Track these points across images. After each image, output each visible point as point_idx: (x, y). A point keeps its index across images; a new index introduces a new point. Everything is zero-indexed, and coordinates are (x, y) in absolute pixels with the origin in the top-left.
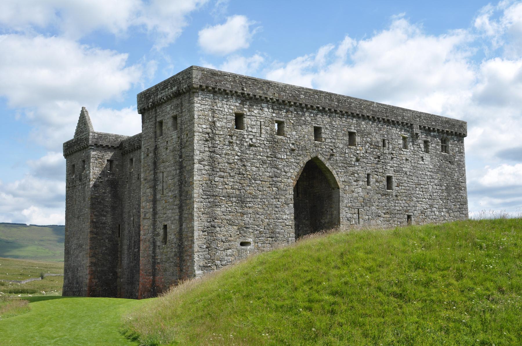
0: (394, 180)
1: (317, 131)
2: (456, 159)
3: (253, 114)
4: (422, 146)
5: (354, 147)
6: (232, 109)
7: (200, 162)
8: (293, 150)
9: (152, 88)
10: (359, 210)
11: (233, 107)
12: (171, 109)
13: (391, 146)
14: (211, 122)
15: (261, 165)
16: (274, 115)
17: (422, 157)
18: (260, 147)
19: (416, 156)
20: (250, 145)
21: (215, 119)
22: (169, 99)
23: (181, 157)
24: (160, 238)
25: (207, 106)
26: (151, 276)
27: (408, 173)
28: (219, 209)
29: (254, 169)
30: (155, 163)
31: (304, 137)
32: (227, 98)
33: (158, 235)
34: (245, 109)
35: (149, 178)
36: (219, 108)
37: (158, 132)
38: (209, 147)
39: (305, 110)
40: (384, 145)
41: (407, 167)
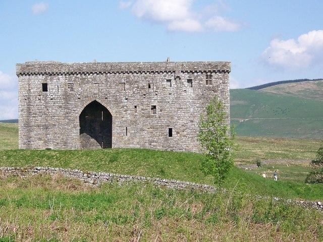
4: (186, 84)
29: (54, 111)
40: (149, 87)
41: (170, 99)
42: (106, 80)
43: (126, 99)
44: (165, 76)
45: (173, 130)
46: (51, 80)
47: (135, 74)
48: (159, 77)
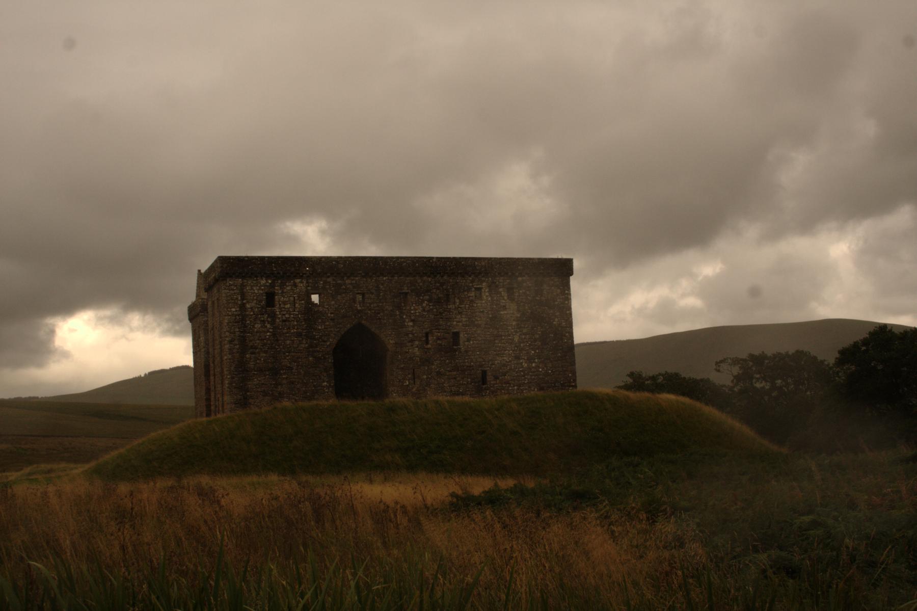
0: (461, 335)
2: (556, 303)
3: (285, 291)
6: (262, 290)
7: (231, 342)
8: (332, 319)
10: (415, 370)
11: (263, 288)
13: (457, 301)
14: (240, 305)
15: (296, 337)
16: (309, 288)
18: (294, 321)
19: (495, 306)
21: (245, 301)
24: (217, 409)
25: (235, 291)
32: (257, 280)
34: (276, 288)
36: (249, 291)
38: (239, 328)
39: (345, 278)
43: (413, 321)
44: (472, 282)
45: (489, 373)
46: (282, 286)
47: (425, 278)
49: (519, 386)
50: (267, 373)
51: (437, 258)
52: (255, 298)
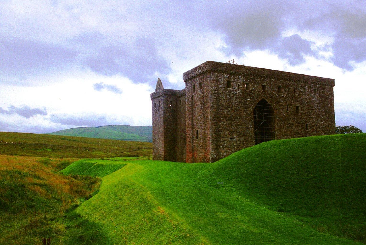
1: (264, 87)
5: (281, 94)
9: (190, 71)
10: (284, 122)
12: (199, 80)
16: (244, 81)
17: (313, 97)
20: (234, 95)
22: (198, 75)
23: (204, 101)
26: (191, 152)
27: (306, 104)
28: (221, 124)
30: (192, 104)
31: (258, 90)
33: (194, 135)
34: (231, 79)
35: (189, 110)
37: (193, 89)
38: (216, 97)
42: (270, 83)
43: (283, 100)
45: (308, 125)
46: (234, 78)
47: (287, 81)
48: (300, 85)
49: (318, 131)
50: (228, 119)
51: (291, 73)
52: (223, 83)
